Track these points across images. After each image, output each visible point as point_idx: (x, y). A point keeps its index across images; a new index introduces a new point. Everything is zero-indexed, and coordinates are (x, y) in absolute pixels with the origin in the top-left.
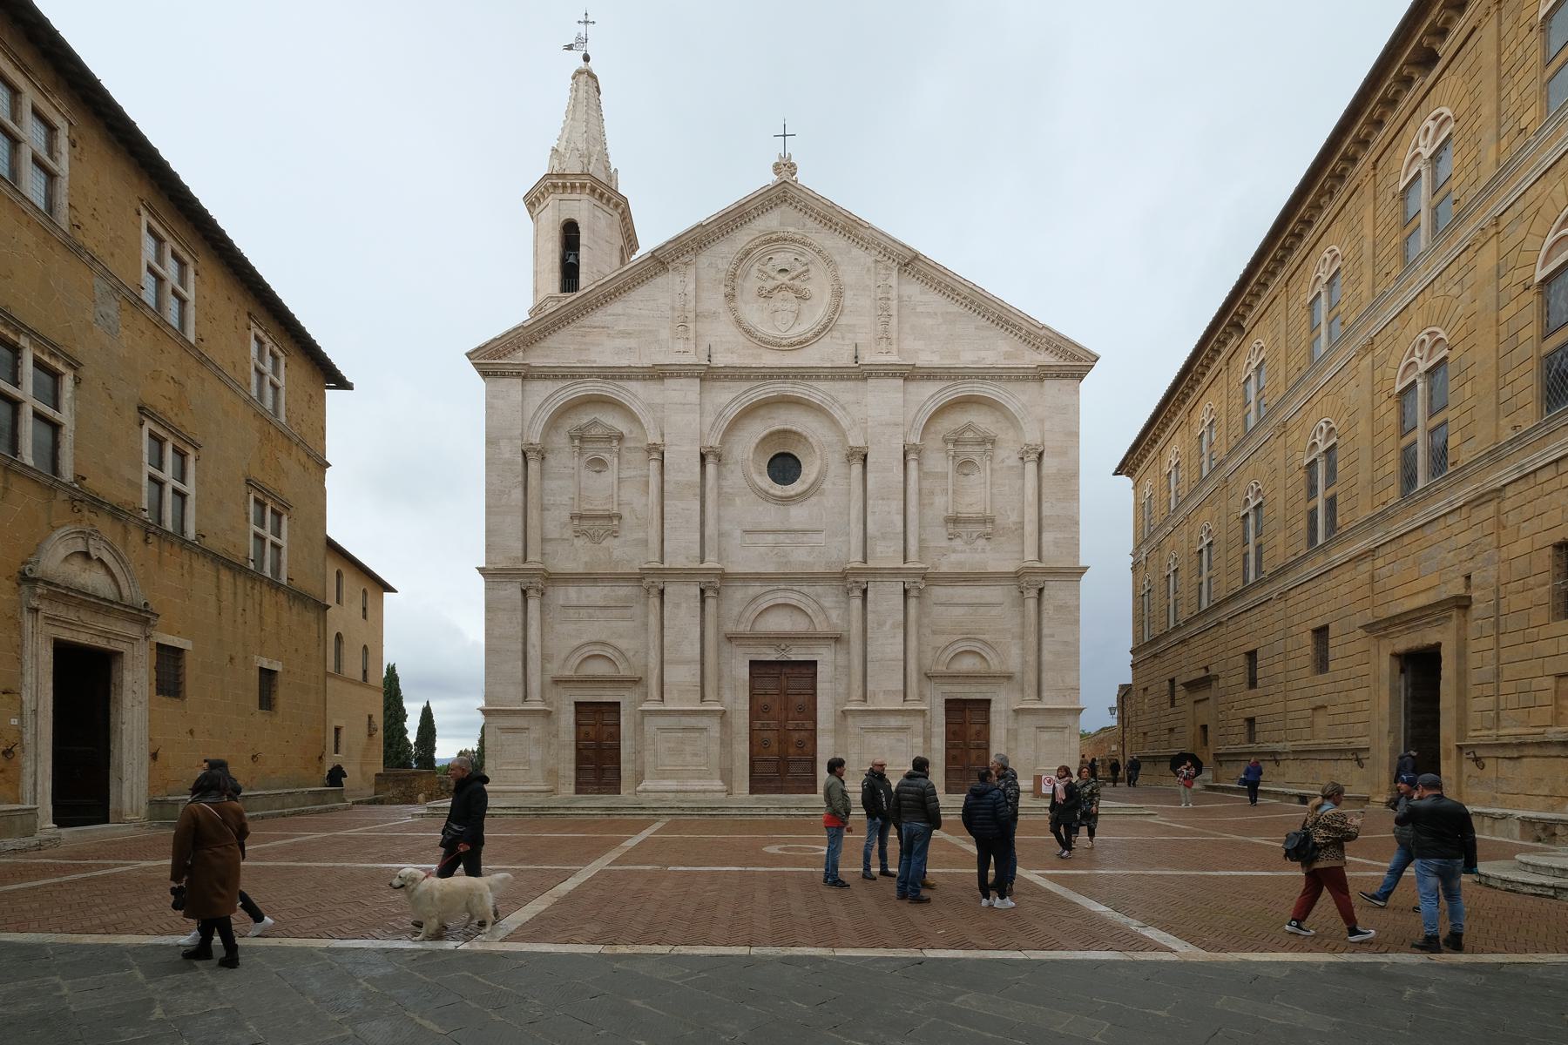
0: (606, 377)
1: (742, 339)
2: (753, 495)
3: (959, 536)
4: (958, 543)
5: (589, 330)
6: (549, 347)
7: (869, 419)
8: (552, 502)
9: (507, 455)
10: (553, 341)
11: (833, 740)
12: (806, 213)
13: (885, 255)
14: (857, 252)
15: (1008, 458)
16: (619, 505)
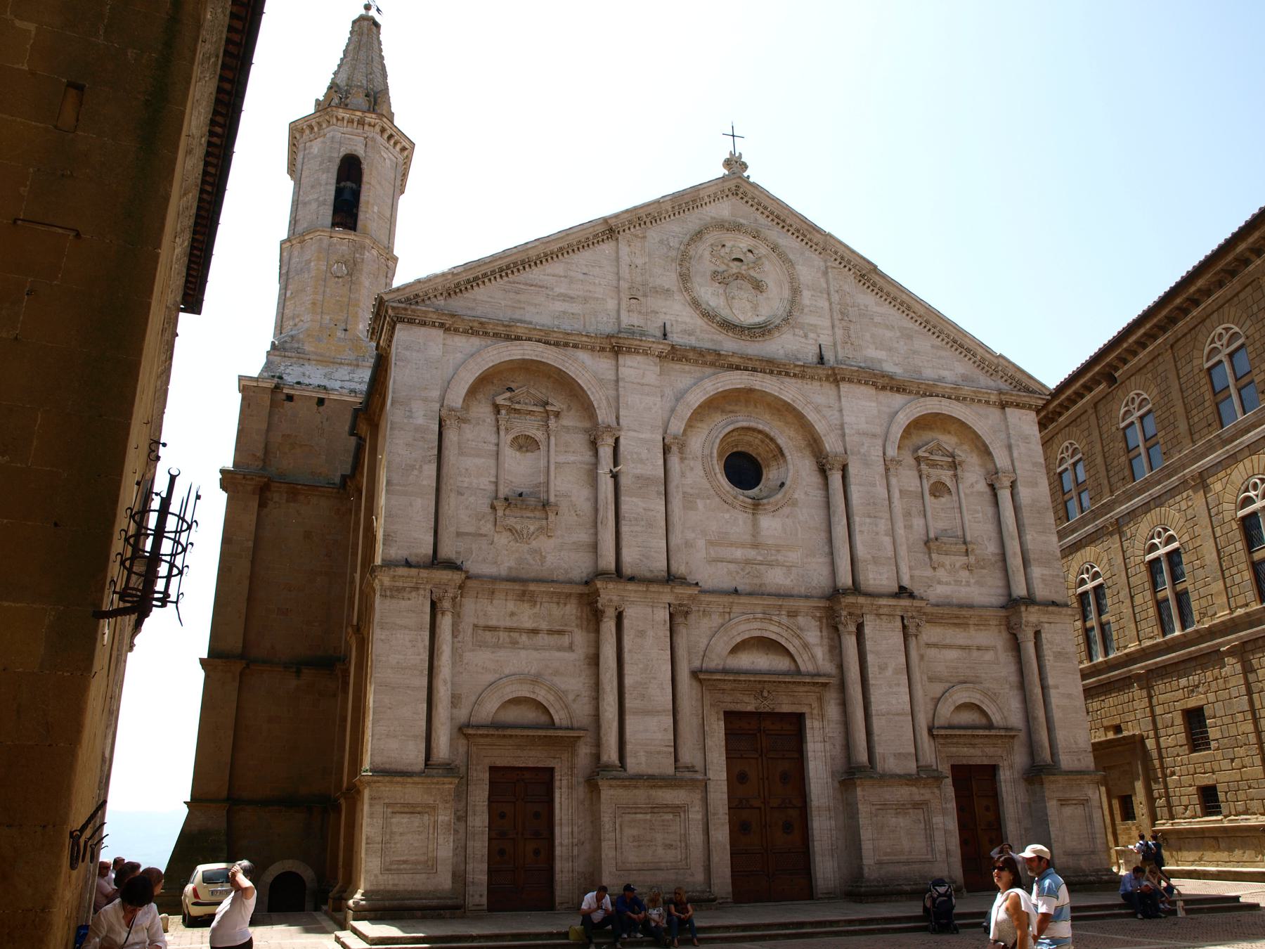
0: (547, 343)
1: (700, 322)
2: (717, 499)
3: (943, 566)
4: (941, 573)
5: (522, 287)
6: (475, 300)
7: (846, 426)
8: (466, 485)
9: (420, 421)
10: (480, 293)
11: (833, 823)
12: (757, 209)
13: (840, 263)
14: (809, 253)
15: (976, 482)
16: (556, 496)
